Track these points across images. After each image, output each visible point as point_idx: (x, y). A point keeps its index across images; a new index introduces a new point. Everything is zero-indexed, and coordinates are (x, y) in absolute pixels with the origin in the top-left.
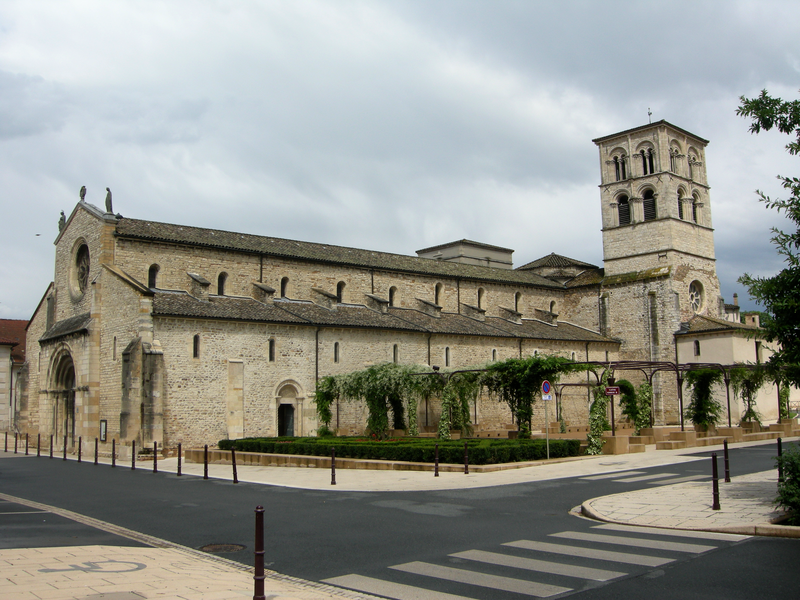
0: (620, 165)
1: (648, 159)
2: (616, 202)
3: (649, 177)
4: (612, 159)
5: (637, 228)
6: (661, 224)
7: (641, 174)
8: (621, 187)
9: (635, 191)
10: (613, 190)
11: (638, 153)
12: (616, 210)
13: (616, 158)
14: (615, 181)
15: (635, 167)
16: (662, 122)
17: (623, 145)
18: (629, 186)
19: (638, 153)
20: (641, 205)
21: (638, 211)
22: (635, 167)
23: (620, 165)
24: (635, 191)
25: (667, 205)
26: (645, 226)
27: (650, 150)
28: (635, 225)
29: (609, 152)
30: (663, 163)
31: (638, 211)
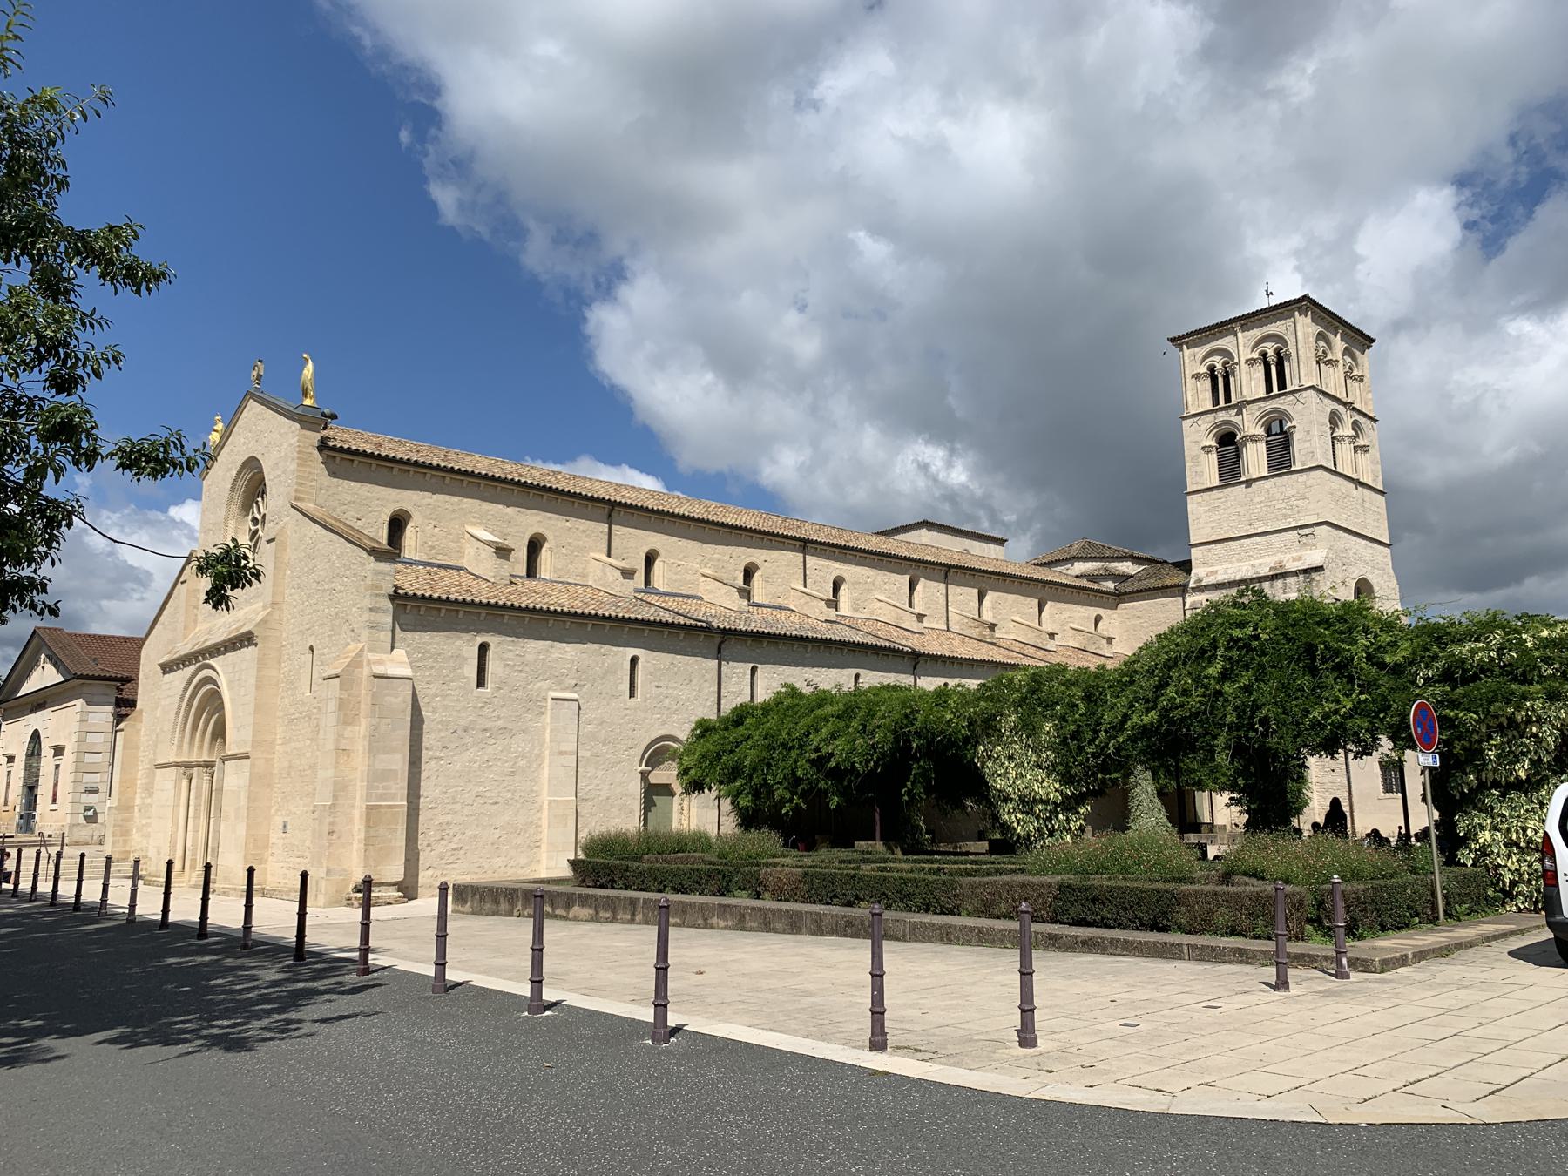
0: (1220, 380)
1: (1276, 368)
2: (1213, 443)
3: (1278, 396)
7: (1262, 394)
8: (1222, 416)
9: (1249, 423)
10: (1206, 423)
11: (1256, 355)
12: (1214, 457)
14: (1210, 407)
15: (1250, 383)
16: (1306, 298)
18: (1240, 413)
19: (1256, 355)
22: (1250, 383)
23: (1220, 380)
24: (1249, 423)
25: (1309, 444)
26: (1271, 482)
30: (1302, 371)
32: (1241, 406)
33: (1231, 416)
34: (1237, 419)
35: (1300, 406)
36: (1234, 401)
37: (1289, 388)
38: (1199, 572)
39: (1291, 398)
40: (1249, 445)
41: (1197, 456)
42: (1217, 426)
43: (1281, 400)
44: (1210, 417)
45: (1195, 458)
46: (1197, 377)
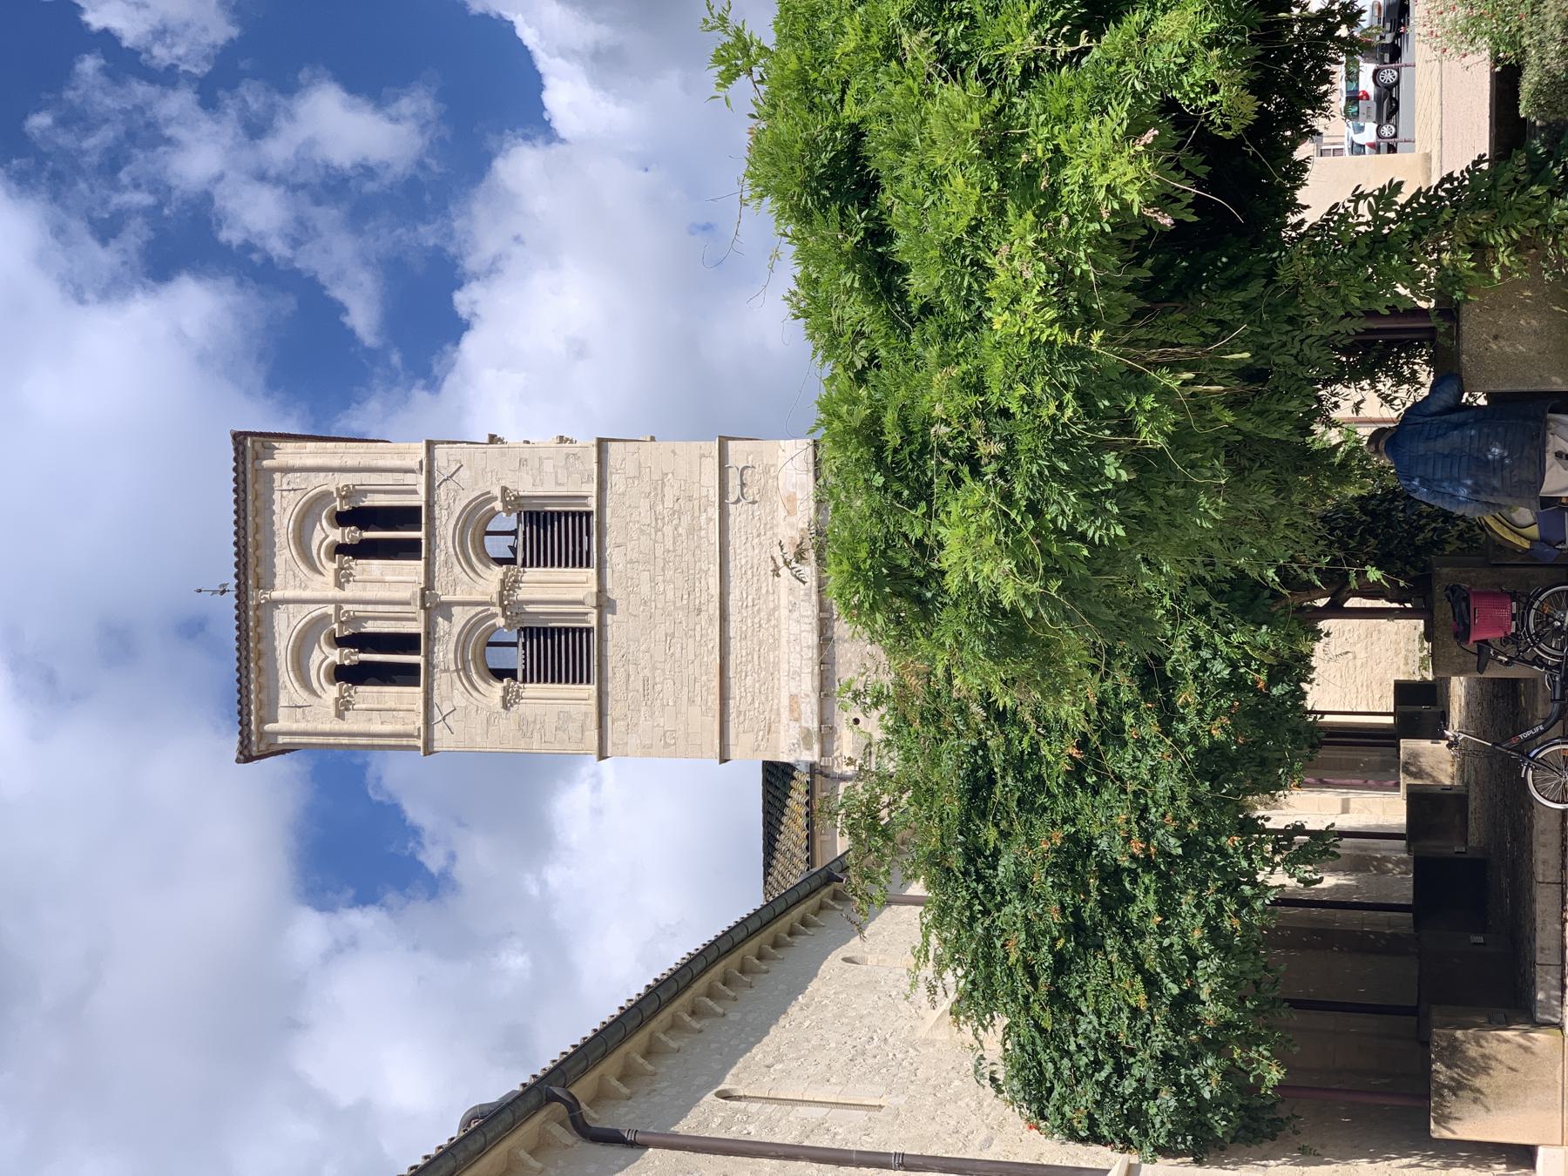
3: (431, 535)
4: (333, 691)
5: (614, 591)
6: (616, 482)
8: (445, 653)
11: (331, 567)
13: (342, 674)
17: (285, 627)
18: (446, 609)
19: (331, 567)
20: (532, 574)
21: (554, 589)
24: (473, 587)
26: (614, 556)
27: (341, 519)
28: (604, 603)
29: (302, 696)
31: (554, 589)
32: (433, 607)
33: (449, 631)
34: (461, 616)
35: (464, 474)
36: (416, 627)
37: (419, 500)
38: (790, 749)
39: (442, 494)
40: (522, 594)
41: (523, 726)
42: (463, 669)
43: (441, 514)
44: (442, 682)
45: (523, 726)
46: (343, 707)
